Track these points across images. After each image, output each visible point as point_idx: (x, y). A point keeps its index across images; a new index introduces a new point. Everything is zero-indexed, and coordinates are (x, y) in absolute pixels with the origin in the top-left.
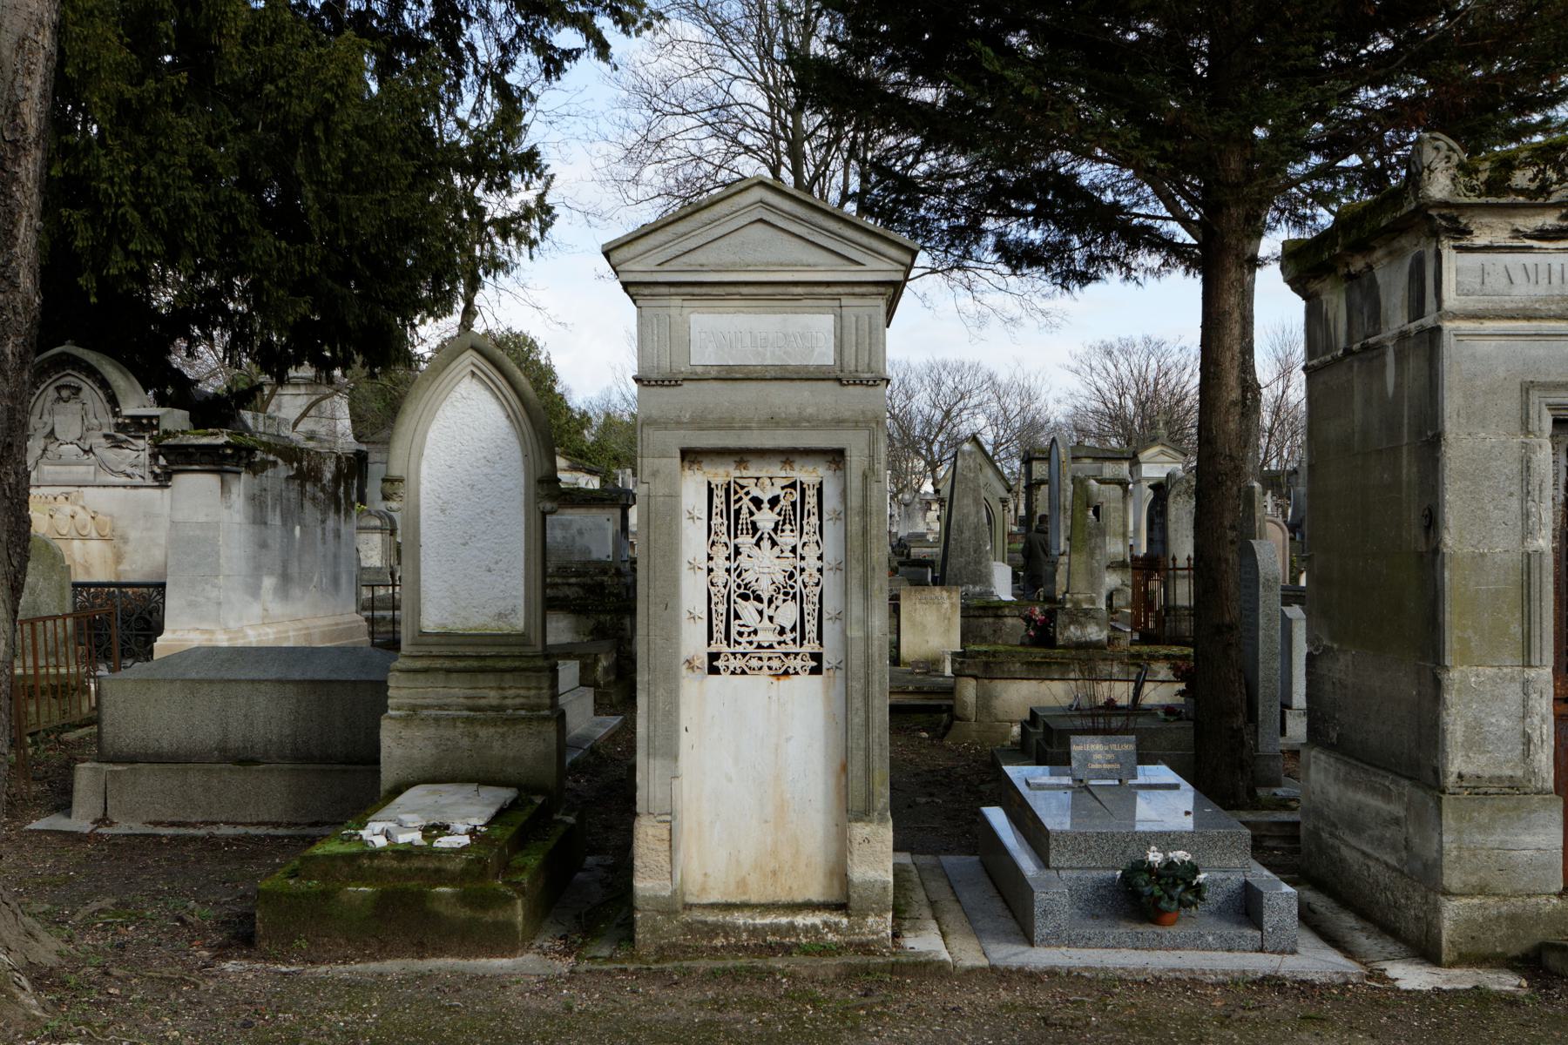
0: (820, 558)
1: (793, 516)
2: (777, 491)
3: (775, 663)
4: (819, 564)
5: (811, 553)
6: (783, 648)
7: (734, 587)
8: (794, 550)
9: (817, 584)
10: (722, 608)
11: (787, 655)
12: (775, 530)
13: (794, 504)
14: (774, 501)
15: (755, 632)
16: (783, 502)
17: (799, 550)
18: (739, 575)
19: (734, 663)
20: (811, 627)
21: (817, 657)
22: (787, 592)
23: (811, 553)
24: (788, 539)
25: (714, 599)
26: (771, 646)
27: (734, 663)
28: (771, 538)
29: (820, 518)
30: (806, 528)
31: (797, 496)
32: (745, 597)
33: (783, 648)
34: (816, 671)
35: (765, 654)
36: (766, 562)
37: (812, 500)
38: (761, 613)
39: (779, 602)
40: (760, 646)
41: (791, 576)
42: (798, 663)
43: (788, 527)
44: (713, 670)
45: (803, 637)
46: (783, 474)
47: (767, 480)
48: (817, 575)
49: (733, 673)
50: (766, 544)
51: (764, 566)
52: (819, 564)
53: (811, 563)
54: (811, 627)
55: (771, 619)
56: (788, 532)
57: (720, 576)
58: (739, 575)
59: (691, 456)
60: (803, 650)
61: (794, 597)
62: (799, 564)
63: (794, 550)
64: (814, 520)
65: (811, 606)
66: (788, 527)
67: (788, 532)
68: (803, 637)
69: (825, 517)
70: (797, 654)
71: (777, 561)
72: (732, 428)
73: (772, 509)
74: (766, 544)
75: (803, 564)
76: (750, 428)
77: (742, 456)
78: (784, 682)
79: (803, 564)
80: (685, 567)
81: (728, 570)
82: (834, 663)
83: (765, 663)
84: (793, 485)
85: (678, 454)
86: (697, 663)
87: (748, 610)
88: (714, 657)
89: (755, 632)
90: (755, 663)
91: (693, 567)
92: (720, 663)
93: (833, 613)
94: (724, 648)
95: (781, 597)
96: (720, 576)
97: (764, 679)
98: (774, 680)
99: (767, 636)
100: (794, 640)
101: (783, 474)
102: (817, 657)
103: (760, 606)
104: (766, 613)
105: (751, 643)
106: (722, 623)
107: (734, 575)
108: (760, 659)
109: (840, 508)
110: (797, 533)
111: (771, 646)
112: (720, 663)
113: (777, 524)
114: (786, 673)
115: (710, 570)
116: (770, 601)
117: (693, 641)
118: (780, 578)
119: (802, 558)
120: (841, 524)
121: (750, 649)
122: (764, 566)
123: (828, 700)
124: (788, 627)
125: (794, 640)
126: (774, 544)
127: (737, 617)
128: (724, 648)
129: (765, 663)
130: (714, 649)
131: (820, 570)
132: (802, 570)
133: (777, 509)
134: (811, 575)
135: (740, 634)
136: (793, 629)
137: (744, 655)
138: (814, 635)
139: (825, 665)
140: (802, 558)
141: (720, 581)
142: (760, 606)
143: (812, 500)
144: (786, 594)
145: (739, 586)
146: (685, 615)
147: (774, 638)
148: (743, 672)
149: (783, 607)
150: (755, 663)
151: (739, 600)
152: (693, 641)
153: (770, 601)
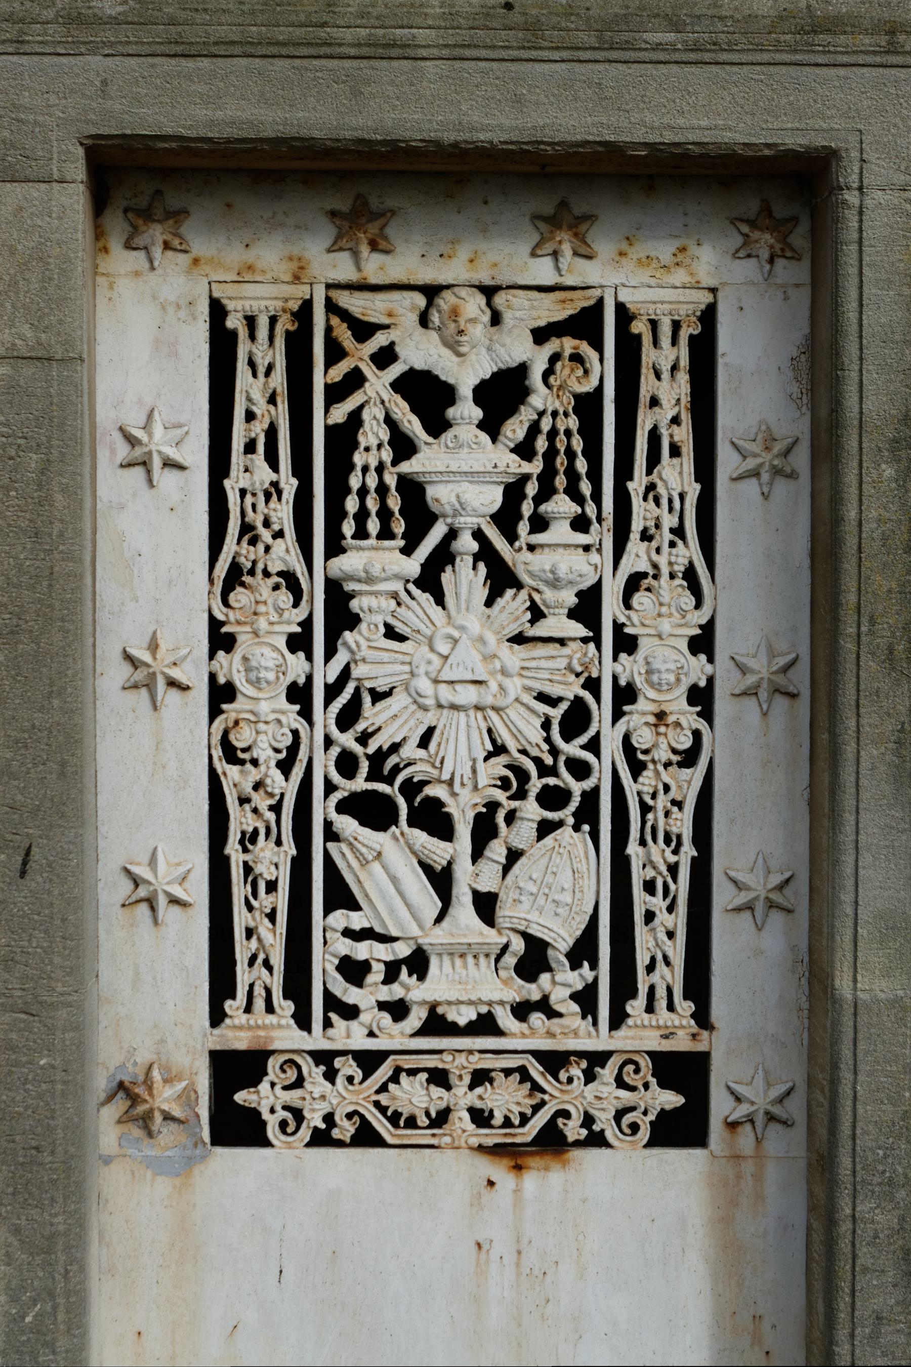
0: (703, 643)
1: (580, 462)
2: (517, 348)
3: (504, 1098)
4: (697, 669)
5: (663, 621)
6: (537, 1035)
7: (324, 765)
8: (587, 607)
9: (689, 758)
10: (274, 860)
11: (554, 1062)
12: (506, 519)
13: (588, 406)
14: (502, 394)
15: (418, 963)
16: (540, 398)
17: (611, 607)
18: (348, 717)
19: (321, 1097)
20: (660, 940)
21: (684, 1071)
22: (556, 783)
23: (663, 621)
24: (561, 558)
25: (240, 820)
26: (485, 1025)
27: (321, 1097)
28: (486, 553)
29: (705, 470)
30: (641, 513)
31: (603, 370)
32: (373, 812)
33: (537, 1035)
34: (679, 1130)
35: (460, 1054)
36: (467, 661)
37: (667, 393)
38: (441, 880)
39: (522, 834)
40: (436, 1024)
41: (576, 720)
42: (602, 1096)
43: (561, 506)
44: (237, 1127)
45: (624, 985)
46: (542, 271)
47: (474, 299)
48: (690, 718)
49: (321, 1138)
50: (466, 580)
51: (458, 677)
52: (697, 669)
53: (664, 662)
54: (660, 940)
55: (486, 906)
56: (560, 532)
57: (265, 718)
58: (348, 717)
59: (140, 183)
60: (623, 1040)
61: (587, 813)
62: (608, 669)
63: (587, 607)
64: (677, 476)
65: (659, 853)
66: (561, 506)
67: (560, 532)
68: (624, 985)
69: (726, 462)
70: (597, 1059)
71: (513, 657)
72: (327, 50)
73: (491, 426)
74: (466, 580)
75: (629, 668)
76: (402, 51)
77: (363, 182)
78: (544, 1182)
79: (629, 668)
80: (112, 675)
81: (299, 694)
82: (759, 1097)
83: (462, 1097)
84: (585, 324)
85: (78, 170)
86: (165, 1097)
87: (387, 868)
88: (236, 1069)
89: (418, 963)
90: (414, 1096)
91: (146, 680)
92: (265, 1098)
93: (759, 885)
94: (284, 1035)
95: (531, 810)
96: (265, 718)
97: (452, 1170)
98: (498, 1170)
99: (465, 983)
100: (586, 999)
101: (542, 271)
102: (684, 1071)
103: (438, 851)
104: (467, 877)
105: (398, 1010)
106: (275, 919)
107: (325, 717)
108: (439, 1078)
109: (794, 425)
110: (602, 534)
111: (485, 1025)
112: (265, 1098)
113: (514, 492)
114: (551, 1141)
115: (221, 694)
116: (484, 830)
117: (149, 999)
118: (526, 729)
119: (626, 643)
120: (794, 500)
121: (395, 1036)
122: (458, 677)
123: (731, 1256)
124: (562, 936)
125: (586, 999)
126: (501, 579)
127: (340, 896)
128: (284, 1035)
129: (462, 1097)
130: (237, 1035)
131: (701, 697)
132: (625, 695)
133: (515, 429)
134: (661, 717)
135: (354, 971)
136: (583, 951)
137: (369, 1061)
138: (672, 976)
139: (720, 1106)
140: (626, 643)
141: (266, 747)
142: (438, 851)
143: (667, 393)
144: (553, 798)
145: (347, 764)
146: (111, 891)
147: (499, 989)
148: (365, 1137)
149: (539, 858)
150: (414, 1096)
151: (347, 825)
152: (149, 999)
153: (484, 830)
